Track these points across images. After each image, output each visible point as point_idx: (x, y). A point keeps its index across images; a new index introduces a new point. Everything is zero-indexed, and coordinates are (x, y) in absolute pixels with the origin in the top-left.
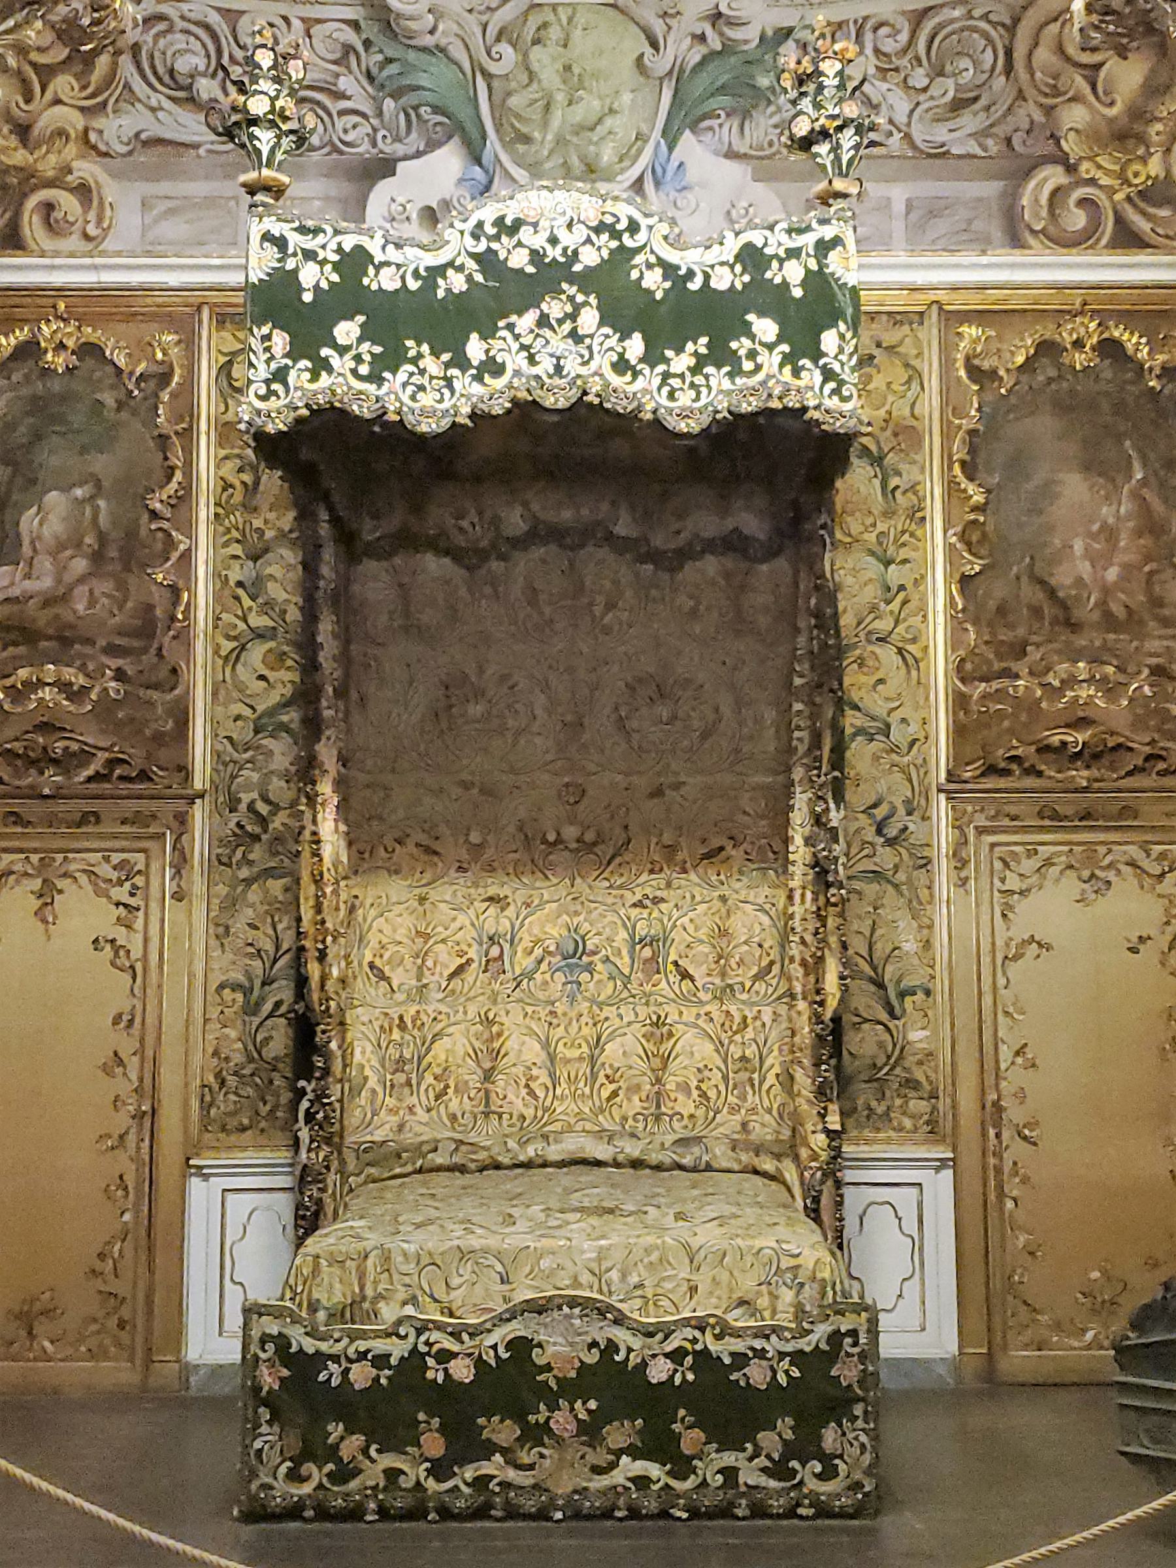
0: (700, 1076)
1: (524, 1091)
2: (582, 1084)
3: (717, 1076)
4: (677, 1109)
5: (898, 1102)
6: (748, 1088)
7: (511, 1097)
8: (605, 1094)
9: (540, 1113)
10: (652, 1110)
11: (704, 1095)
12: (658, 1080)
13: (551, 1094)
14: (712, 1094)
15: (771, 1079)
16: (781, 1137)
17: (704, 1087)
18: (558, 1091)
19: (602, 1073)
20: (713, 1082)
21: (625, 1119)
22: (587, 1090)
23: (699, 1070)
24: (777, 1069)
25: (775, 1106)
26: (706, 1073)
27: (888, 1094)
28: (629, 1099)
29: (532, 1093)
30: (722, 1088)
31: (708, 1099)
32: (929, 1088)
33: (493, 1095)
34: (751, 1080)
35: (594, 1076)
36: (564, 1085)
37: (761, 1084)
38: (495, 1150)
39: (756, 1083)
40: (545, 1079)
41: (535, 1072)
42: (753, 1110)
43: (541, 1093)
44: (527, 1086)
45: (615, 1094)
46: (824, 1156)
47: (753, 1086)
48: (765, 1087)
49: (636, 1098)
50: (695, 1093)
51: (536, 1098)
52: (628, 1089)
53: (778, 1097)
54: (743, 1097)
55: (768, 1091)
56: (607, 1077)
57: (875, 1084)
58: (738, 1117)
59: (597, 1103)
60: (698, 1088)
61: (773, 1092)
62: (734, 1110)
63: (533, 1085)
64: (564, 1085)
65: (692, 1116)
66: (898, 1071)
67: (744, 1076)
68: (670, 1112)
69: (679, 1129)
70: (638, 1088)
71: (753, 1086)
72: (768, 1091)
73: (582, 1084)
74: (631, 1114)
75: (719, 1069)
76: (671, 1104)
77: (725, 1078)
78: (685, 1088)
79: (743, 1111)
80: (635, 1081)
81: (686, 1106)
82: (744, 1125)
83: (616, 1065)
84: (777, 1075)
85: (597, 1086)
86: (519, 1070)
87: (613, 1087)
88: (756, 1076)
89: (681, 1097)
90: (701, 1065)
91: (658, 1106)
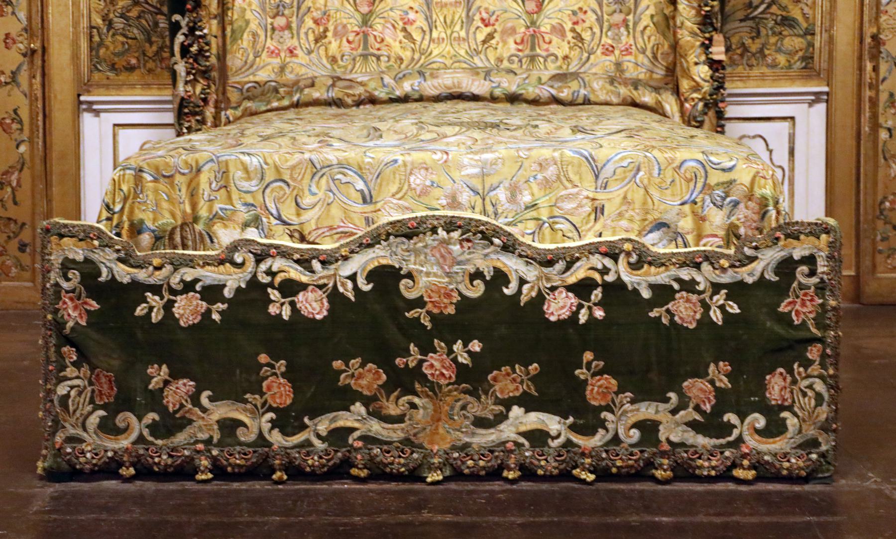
0: (575, 19)
1: (401, 35)
2: (457, 28)
3: (591, 18)
4: (553, 50)
5: (773, 40)
6: (623, 30)
7: (389, 40)
8: (481, 37)
9: (417, 56)
10: (527, 52)
11: (579, 37)
12: (533, 23)
13: (427, 37)
14: (586, 36)
15: (646, 21)
16: (655, 76)
17: (578, 29)
18: (435, 34)
19: (477, 17)
20: (587, 24)
21: (500, 60)
22: (463, 34)
23: (574, 13)
24: (652, 11)
25: (649, 47)
26: (581, 15)
27: (763, 32)
28: (505, 42)
29: (409, 36)
30: (597, 30)
31: (582, 40)
32: (804, 25)
33: (371, 39)
34: (625, 22)
35: (470, 19)
36: (440, 29)
37: (635, 24)
38: (372, 85)
39: (631, 24)
40: (421, 22)
41: (412, 16)
42: (627, 51)
43: (417, 36)
44: (404, 30)
45: (491, 36)
46: (707, 87)
47: (627, 26)
48: (640, 27)
49: (511, 41)
50: (570, 35)
51: (413, 41)
52: (504, 32)
53: (652, 38)
54: (617, 38)
55: (643, 32)
56: (483, 20)
57: (750, 23)
58: (612, 58)
59: (473, 46)
60: (573, 30)
61: (648, 32)
62: (609, 50)
63: (409, 28)
64: (440, 29)
65: (566, 57)
66: (774, 9)
67: (618, 18)
68: (544, 54)
69: (552, 68)
70: (513, 31)
71: (627, 26)
72: (643, 32)
73: (457, 28)
74: (506, 55)
75: (594, 11)
76: (545, 46)
77: (600, 20)
78: (559, 30)
79: (617, 52)
80: (510, 25)
81: (560, 47)
82: (618, 65)
83: (492, 8)
84: (652, 16)
85: (472, 29)
86: (396, 15)
87: (489, 29)
88: (630, 17)
89: (556, 40)
90: (575, 8)
91: (533, 48)
